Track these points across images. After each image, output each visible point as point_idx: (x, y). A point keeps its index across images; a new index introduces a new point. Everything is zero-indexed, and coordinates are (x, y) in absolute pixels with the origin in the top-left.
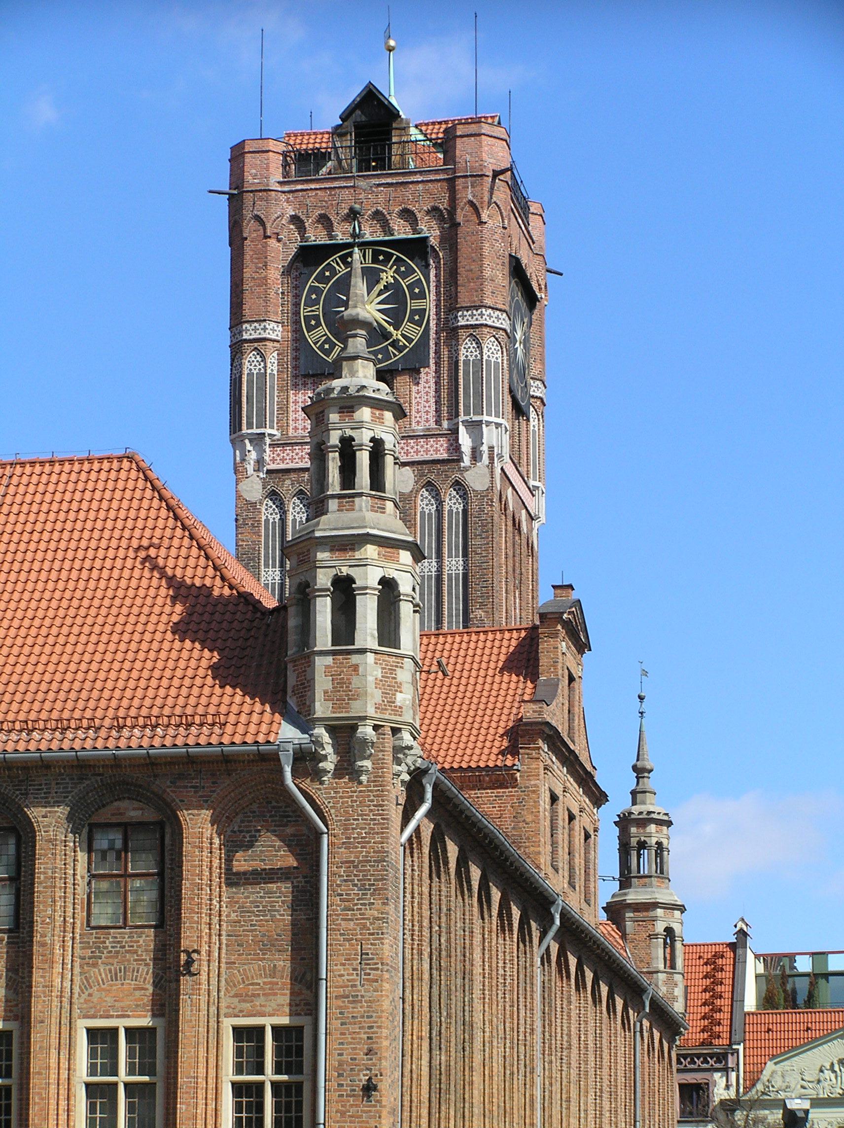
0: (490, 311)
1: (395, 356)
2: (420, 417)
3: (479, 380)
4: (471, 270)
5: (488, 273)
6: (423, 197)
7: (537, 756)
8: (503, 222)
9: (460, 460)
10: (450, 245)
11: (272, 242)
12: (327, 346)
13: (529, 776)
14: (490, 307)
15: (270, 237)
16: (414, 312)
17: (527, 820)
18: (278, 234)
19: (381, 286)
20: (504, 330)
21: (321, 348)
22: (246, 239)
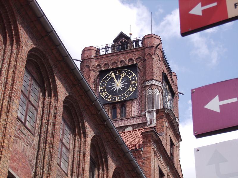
0: (155, 81)
1: (127, 96)
2: (135, 113)
3: (152, 99)
4: (150, 71)
5: (155, 71)
6: (135, 56)
7: (150, 145)
8: (159, 59)
9: (146, 123)
10: (144, 66)
11: (92, 72)
12: (106, 96)
13: (147, 153)
14: (155, 80)
15: (91, 70)
16: (132, 84)
17: (146, 170)
18: (93, 70)
19: (121, 78)
20: (160, 87)
21: (105, 97)
22: (84, 71)
